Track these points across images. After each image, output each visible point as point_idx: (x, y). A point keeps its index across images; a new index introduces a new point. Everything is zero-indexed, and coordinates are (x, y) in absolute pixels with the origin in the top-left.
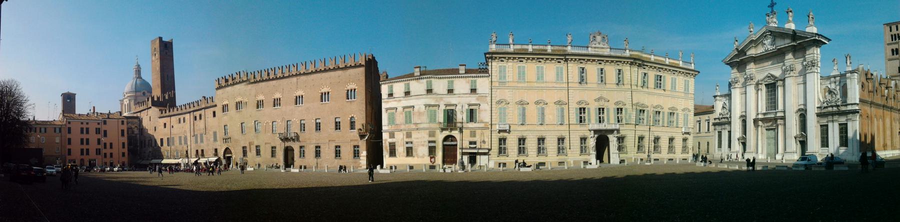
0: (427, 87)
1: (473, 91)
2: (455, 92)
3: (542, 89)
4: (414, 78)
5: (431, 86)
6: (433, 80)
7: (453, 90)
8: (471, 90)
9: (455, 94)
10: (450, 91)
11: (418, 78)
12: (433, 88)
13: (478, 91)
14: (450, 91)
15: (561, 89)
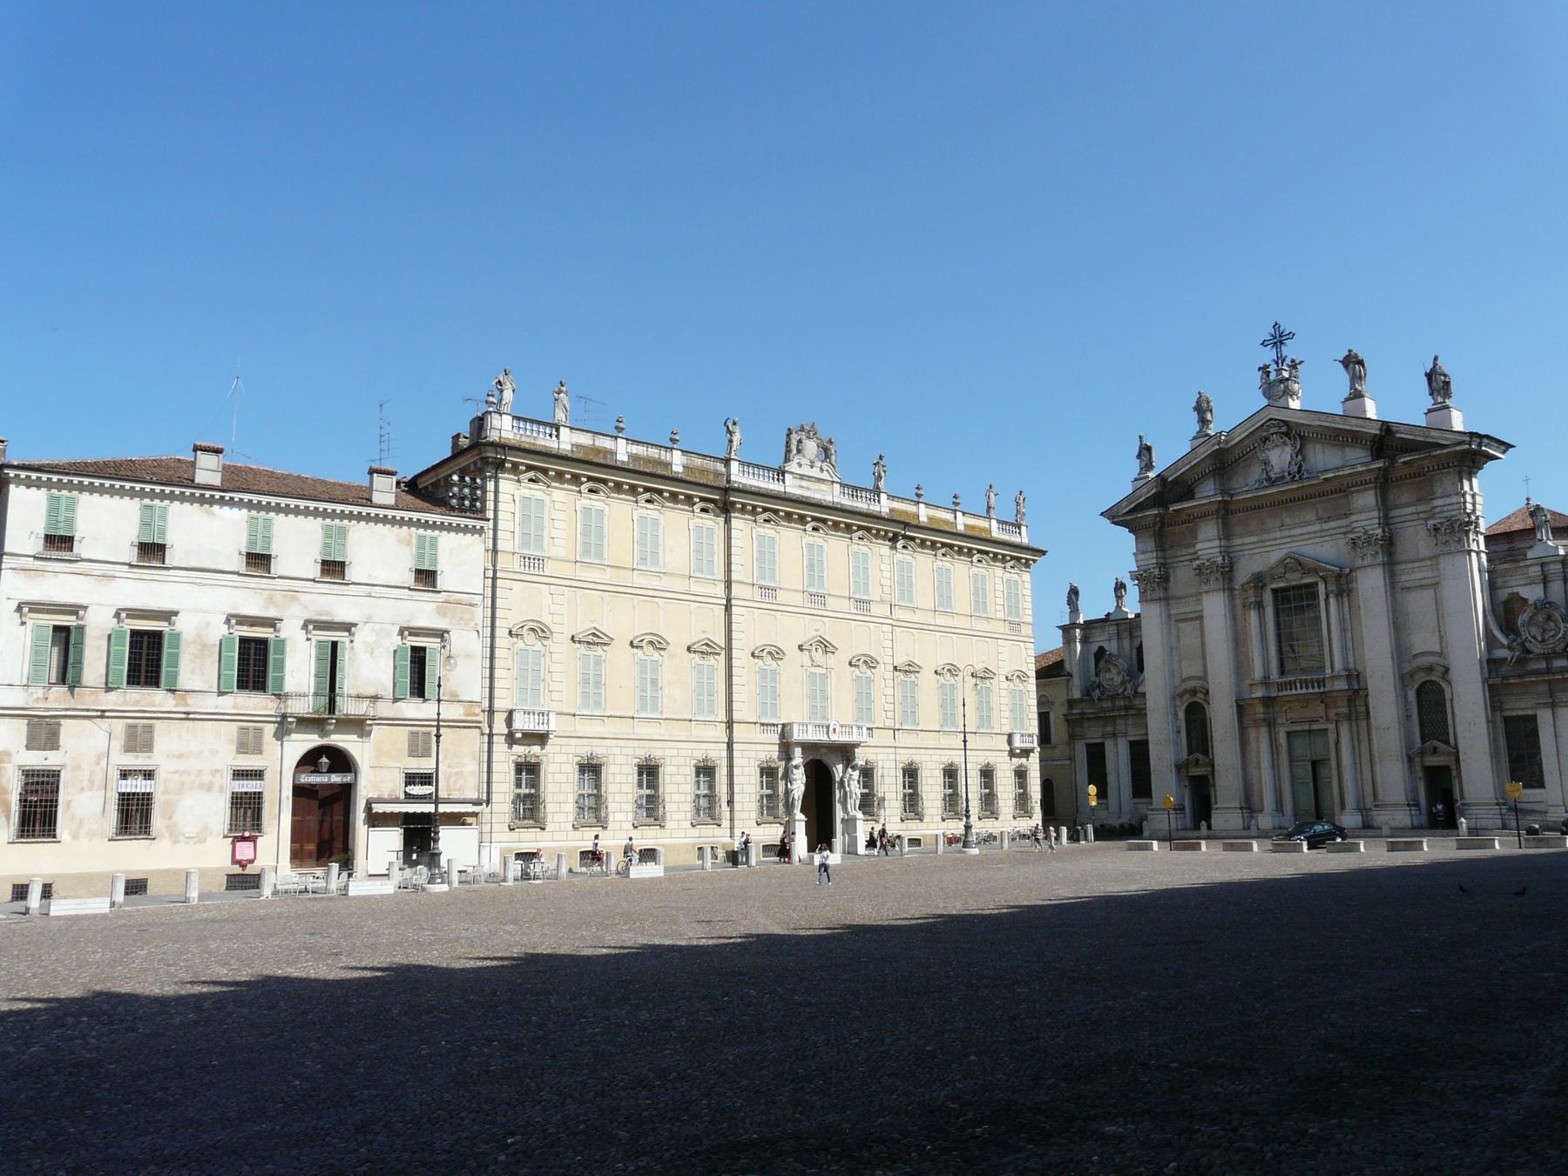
0: (252, 543)
1: (426, 577)
2: (352, 574)
3: (652, 595)
4: (188, 492)
5: (268, 539)
6: (175, 508)
7: (342, 564)
8: (324, 563)
9: (439, 592)
10: (333, 569)
11: (206, 497)
12: (168, 543)
13: (441, 582)
14: (333, 569)
15: (704, 600)
